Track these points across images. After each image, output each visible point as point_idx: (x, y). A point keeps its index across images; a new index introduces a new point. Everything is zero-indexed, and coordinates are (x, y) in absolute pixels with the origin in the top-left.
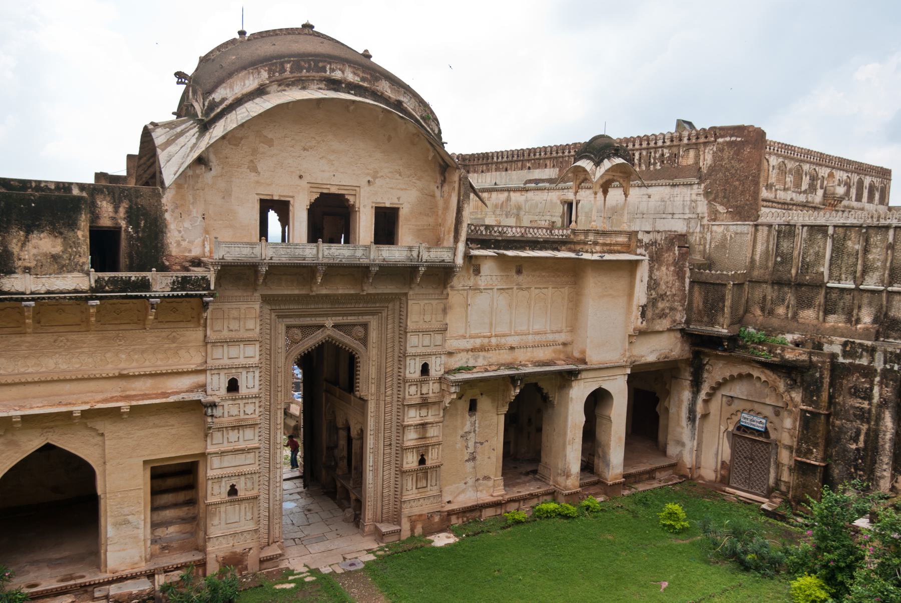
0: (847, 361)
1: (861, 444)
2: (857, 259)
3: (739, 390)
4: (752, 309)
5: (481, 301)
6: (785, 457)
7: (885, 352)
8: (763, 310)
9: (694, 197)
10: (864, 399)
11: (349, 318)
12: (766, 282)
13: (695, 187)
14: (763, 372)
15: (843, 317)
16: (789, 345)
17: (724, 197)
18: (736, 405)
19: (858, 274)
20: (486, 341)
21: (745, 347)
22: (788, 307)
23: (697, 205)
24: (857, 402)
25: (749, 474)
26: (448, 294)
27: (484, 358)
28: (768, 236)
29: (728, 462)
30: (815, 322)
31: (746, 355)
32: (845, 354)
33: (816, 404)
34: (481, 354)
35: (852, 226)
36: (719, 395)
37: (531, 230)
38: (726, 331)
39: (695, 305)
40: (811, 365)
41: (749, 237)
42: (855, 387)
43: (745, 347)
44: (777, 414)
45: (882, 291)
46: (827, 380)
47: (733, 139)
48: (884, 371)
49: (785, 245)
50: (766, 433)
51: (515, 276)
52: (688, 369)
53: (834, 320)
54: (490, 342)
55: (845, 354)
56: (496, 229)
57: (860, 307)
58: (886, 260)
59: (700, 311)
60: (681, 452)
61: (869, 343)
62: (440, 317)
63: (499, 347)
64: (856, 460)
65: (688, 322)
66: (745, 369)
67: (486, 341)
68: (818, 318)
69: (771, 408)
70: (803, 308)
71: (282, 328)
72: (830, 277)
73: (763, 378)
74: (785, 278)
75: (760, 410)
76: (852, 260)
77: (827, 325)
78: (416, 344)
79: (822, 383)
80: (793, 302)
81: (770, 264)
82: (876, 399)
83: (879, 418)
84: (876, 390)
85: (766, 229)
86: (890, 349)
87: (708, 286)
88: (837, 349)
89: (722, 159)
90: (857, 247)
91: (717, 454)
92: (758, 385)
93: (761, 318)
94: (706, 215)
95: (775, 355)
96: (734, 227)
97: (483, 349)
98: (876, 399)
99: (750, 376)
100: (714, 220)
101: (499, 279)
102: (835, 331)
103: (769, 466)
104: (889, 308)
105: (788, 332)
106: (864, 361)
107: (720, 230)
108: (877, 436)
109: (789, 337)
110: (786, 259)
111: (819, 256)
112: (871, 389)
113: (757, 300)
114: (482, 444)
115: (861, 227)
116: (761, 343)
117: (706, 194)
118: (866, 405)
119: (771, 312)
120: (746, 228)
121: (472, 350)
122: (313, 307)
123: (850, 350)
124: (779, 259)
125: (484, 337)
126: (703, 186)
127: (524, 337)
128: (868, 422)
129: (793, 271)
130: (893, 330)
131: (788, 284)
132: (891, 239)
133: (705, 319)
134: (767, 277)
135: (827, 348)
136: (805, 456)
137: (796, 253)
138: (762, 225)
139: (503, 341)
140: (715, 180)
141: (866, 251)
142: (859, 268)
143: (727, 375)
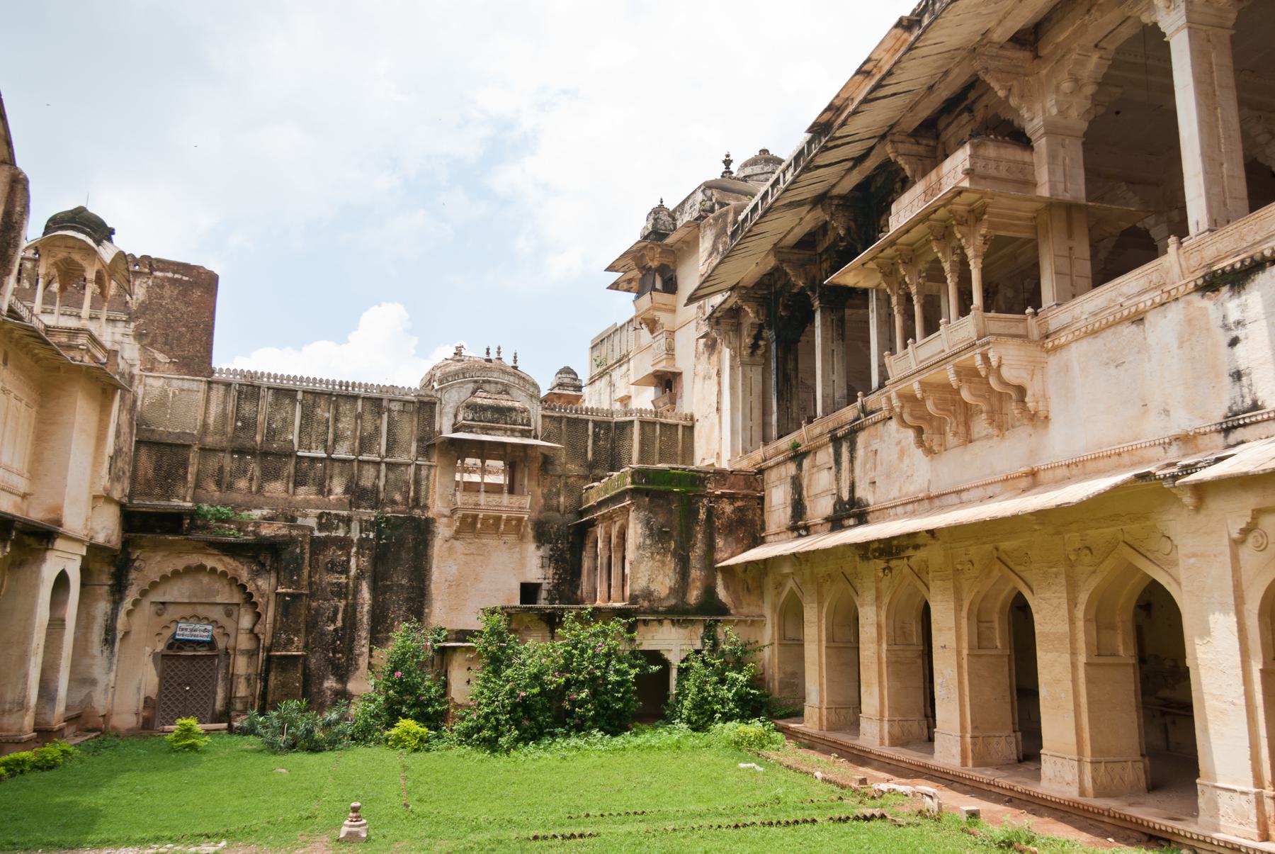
0: (323, 534)
1: (339, 624)
2: (328, 428)
3: (176, 592)
4: (204, 483)
6: (241, 665)
7: (361, 521)
8: (219, 483)
9: (118, 337)
10: (341, 573)
12: (223, 450)
13: (121, 325)
14: (220, 560)
15: (314, 489)
16: (259, 520)
17: (165, 344)
18: (171, 613)
19: (330, 443)
21: (206, 527)
22: (251, 479)
23: (122, 348)
24: (333, 578)
25: (185, 706)
28: (225, 397)
29: (154, 697)
30: (285, 495)
31: (211, 537)
32: (321, 527)
33: (297, 584)
35: (321, 394)
36: (146, 603)
38: (190, 504)
39: (141, 473)
40: (291, 541)
41: (201, 396)
42: (332, 562)
43: (206, 527)
44: (229, 614)
45: (352, 461)
46: (307, 556)
47: (177, 276)
48: (361, 540)
49: (247, 409)
50: (211, 644)
52: (106, 569)
53: (305, 493)
55: (321, 527)
57: (331, 478)
58: (356, 429)
59: (148, 481)
60: (89, 695)
61: (345, 513)
64: (334, 642)
65: (131, 496)
66: (194, 559)
68: (287, 491)
69: (220, 609)
70: (268, 480)
72: (300, 446)
73: (220, 568)
74: (248, 445)
75: (205, 614)
76: (322, 428)
77: (299, 498)
79: (303, 559)
80: (257, 473)
81: (229, 429)
82: (353, 572)
83: (357, 591)
84: (353, 561)
85: (222, 388)
86: (365, 518)
87: (158, 453)
88: (312, 522)
89: (162, 297)
90: (327, 415)
91: (139, 689)
92: (205, 580)
93: (217, 494)
94: (138, 363)
95: (246, 533)
96: (180, 383)
98: (353, 572)
99: (201, 568)
100: (151, 370)
102: (308, 504)
103: (216, 686)
104: (359, 477)
105: (255, 508)
106: (341, 533)
107: (159, 383)
108: (355, 610)
109: (256, 514)
110: (249, 425)
111: (287, 423)
112: (348, 561)
113: (211, 472)
115: (330, 394)
116: (228, 520)
117: (139, 336)
118: (343, 579)
119: (230, 487)
120: (196, 385)
123: (326, 521)
124: (239, 424)
126: (132, 325)
128: (346, 598)
129: (258, 438)
130: (363, 499)
131: (253, 452)
132: (360, 409)
133: (157, 491)
134: (225, 444)
135: (300, 521)
136: (285, 648)
137: (260, 418)
138: (217, 382)
140: (152, 322)
141: (336, 420)
142: (331, 436)
143: (168, 570)
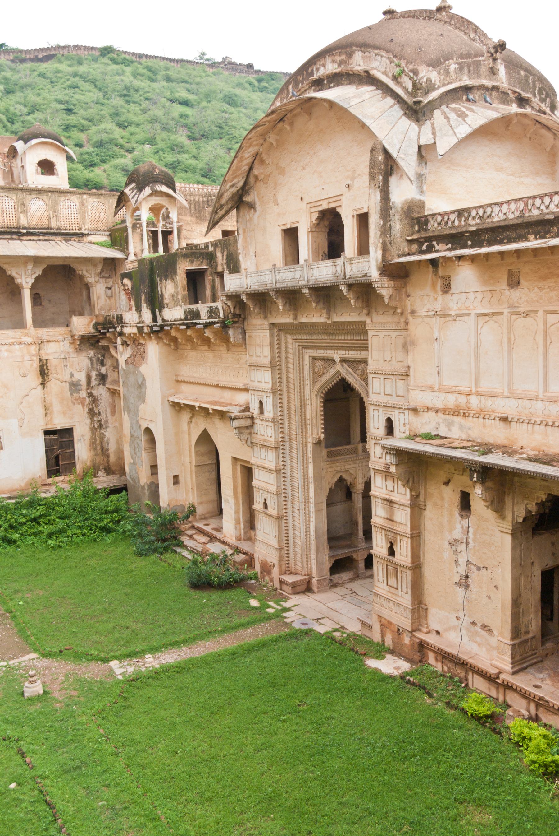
5: (459, 334)
11: (351, 352)
20: (462, 400)
26: (407, 323)
27: (461, 427)
34: (457, 419)
37: (538, 202)
51: (507, 292)
54: (468, 402)
56: (473, 213)
62: (400, 355)
63: (482, 414)
67: (462, 400)
71: (307, 361)
78: (378, 392)
97: (455, 412)
101: (479, 296)
114: (479, 569)
121: (445, 411)
122: (316, 338)
125: (460, 393)
127: (527, 403)
139: (488, 404)
